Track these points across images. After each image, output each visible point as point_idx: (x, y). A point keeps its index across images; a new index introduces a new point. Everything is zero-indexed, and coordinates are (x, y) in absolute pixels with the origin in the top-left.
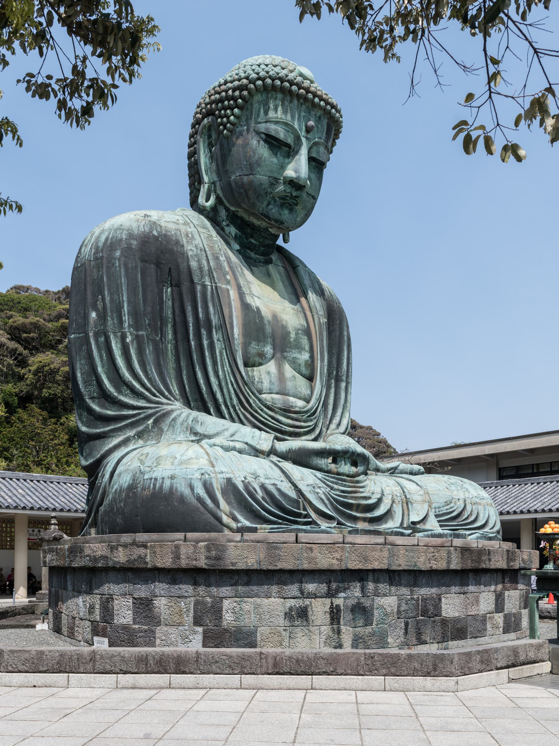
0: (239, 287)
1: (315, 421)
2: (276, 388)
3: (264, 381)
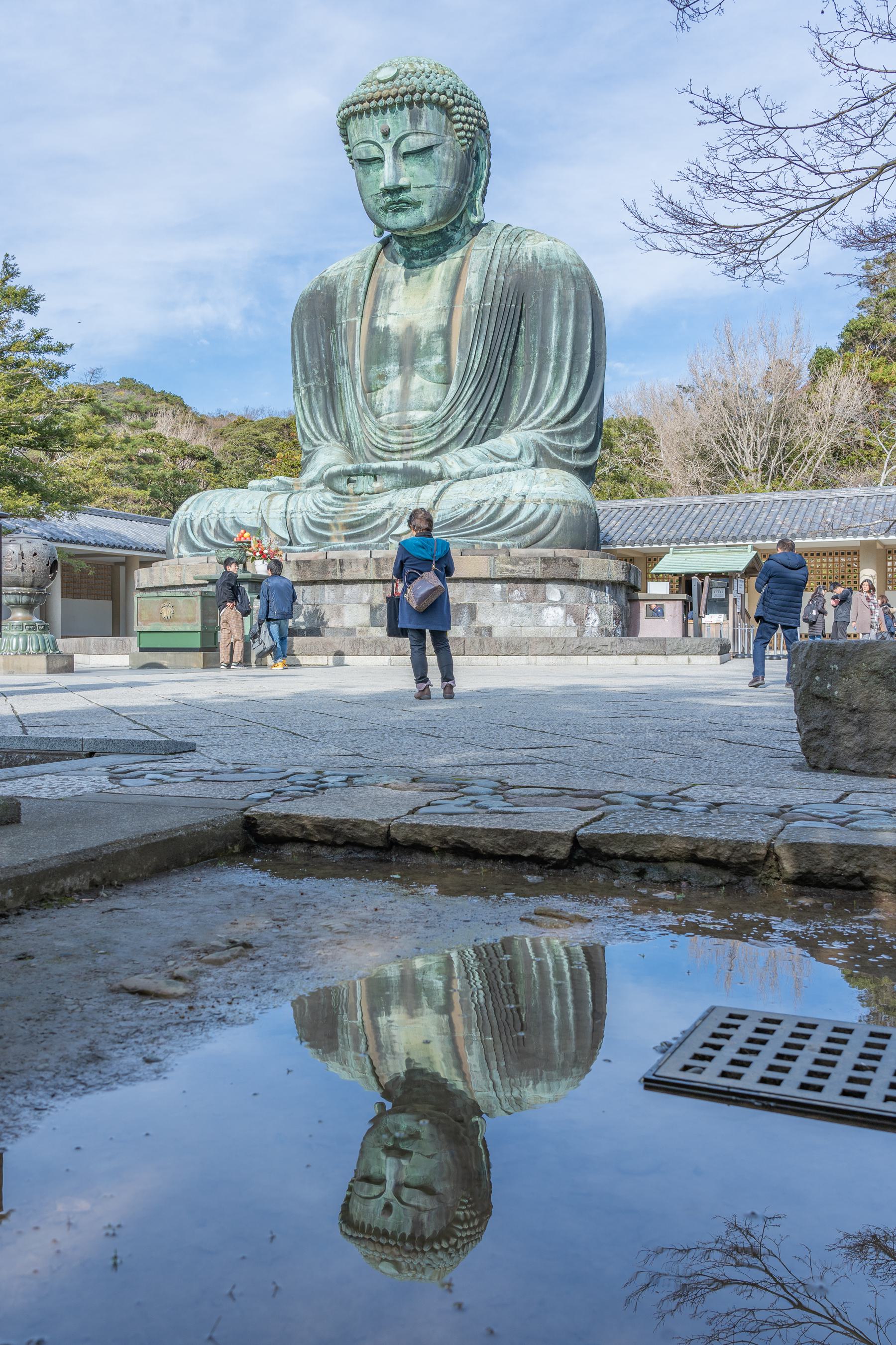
0: (374, 311)
1: (440, 430)
2: (395, 407)
3: (384, 402)
